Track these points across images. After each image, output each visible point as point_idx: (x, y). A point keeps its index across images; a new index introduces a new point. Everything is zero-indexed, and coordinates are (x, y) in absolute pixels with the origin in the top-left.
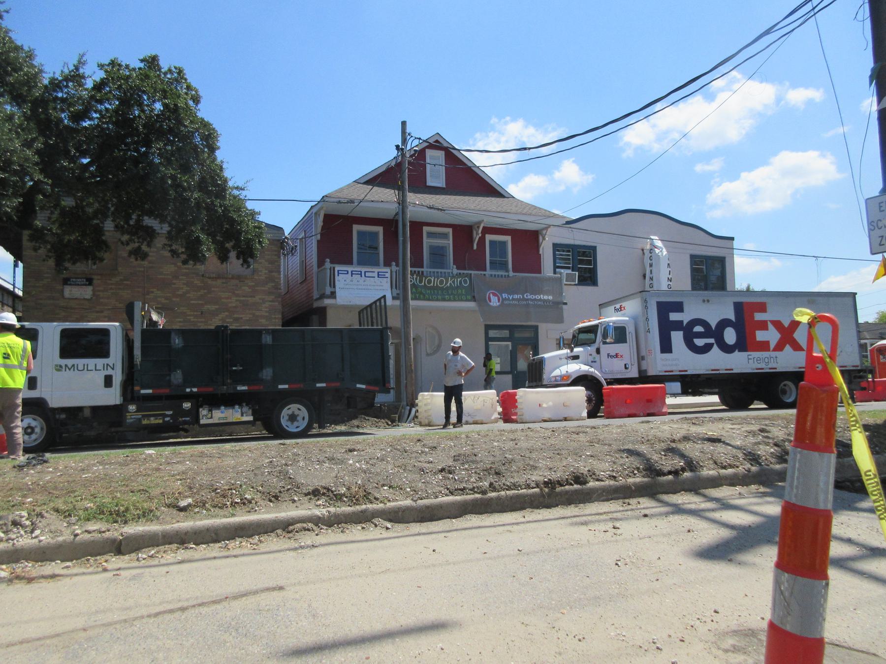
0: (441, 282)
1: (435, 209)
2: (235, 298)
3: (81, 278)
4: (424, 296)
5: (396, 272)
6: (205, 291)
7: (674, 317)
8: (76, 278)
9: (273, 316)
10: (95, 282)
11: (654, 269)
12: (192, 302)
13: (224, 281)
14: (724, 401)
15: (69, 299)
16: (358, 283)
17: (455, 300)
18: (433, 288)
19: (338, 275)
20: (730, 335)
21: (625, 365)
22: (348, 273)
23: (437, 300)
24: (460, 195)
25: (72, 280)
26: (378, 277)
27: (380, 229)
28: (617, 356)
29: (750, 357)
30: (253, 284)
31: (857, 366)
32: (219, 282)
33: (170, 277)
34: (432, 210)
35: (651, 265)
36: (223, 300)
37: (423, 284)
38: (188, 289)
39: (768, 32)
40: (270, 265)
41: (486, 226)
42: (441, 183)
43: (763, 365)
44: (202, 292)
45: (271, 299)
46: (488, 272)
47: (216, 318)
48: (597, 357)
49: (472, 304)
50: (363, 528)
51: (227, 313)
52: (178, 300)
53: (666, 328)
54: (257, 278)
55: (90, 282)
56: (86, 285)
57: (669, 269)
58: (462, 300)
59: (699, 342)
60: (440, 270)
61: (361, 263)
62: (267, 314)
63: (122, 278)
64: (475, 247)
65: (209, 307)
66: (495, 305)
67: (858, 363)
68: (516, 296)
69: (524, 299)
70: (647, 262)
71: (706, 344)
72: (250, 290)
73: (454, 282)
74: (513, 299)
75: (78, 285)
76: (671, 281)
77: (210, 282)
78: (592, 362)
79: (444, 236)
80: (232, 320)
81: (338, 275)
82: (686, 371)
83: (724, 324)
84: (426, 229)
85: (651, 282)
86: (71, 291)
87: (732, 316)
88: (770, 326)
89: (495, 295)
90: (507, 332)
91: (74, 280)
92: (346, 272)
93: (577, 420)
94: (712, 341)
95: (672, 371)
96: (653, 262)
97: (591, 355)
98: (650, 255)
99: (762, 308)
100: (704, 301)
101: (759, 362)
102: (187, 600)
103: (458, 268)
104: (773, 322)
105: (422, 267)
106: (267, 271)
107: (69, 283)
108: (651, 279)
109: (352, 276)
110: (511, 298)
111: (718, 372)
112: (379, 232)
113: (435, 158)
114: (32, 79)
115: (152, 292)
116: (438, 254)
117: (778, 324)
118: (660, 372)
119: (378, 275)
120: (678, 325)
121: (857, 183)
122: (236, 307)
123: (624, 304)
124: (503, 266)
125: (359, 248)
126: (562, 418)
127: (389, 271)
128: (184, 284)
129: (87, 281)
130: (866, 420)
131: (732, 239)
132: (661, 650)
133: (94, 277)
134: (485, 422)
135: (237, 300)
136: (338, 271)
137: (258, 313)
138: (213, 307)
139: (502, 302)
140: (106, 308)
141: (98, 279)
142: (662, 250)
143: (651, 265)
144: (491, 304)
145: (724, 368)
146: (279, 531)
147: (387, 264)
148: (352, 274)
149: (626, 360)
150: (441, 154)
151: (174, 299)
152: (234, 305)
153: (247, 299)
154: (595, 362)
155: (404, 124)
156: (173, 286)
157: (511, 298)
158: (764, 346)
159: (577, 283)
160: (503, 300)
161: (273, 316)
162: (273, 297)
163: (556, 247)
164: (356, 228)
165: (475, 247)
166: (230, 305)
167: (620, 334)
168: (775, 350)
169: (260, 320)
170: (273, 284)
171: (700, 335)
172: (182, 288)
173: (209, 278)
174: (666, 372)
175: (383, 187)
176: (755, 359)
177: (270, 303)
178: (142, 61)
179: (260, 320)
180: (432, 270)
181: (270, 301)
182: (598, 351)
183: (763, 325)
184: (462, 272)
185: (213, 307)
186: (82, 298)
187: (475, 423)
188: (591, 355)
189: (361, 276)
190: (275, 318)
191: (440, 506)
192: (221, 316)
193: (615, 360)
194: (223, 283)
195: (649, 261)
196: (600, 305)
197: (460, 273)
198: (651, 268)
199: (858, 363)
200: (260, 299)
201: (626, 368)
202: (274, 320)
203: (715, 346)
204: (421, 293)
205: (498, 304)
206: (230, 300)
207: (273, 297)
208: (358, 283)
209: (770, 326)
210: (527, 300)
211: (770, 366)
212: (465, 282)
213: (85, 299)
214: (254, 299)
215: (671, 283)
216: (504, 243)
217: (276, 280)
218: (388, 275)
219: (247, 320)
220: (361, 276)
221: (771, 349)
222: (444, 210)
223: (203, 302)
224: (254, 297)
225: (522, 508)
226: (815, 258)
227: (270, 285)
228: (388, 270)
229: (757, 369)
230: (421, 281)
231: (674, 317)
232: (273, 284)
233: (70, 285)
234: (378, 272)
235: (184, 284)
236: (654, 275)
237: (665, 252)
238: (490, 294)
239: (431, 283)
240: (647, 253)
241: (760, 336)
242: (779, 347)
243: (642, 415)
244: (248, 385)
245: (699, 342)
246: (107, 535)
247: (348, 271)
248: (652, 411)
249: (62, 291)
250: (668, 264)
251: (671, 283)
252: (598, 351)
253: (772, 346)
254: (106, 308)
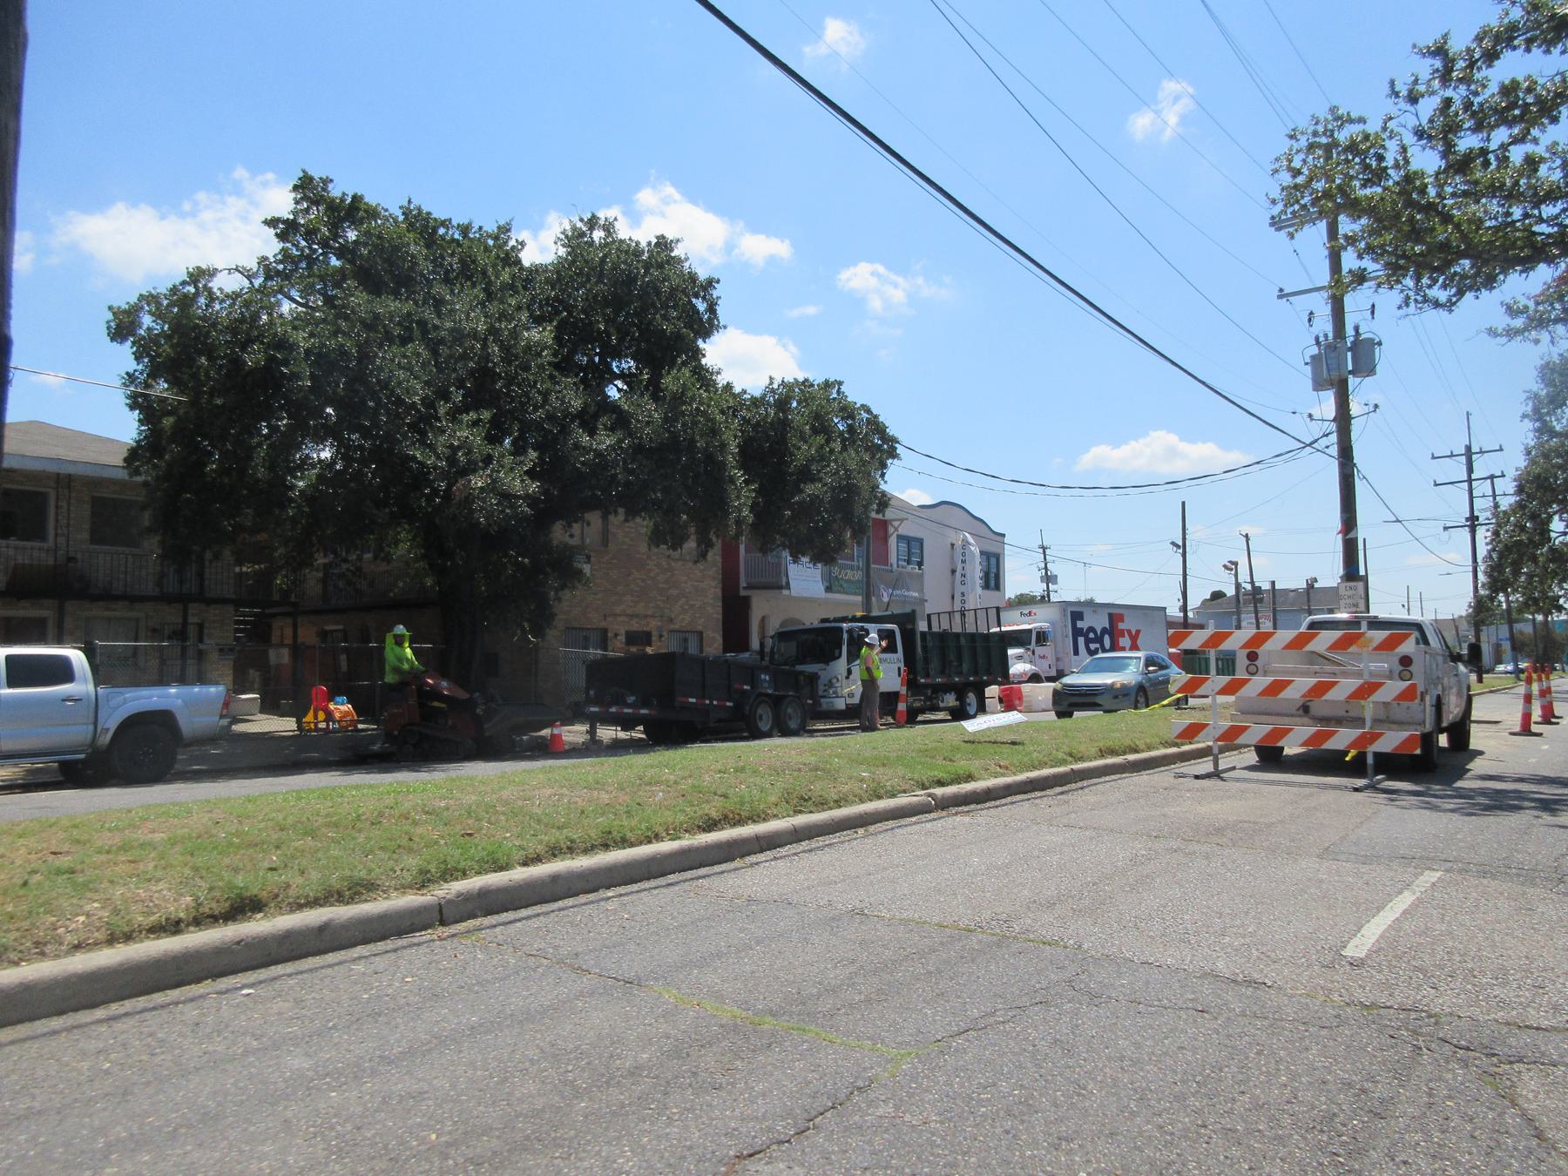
11: (967, 566)
12: (661, 586)
20: (1107, 641)
35: (963, 562)
53: (1077, 632)
70: (959, 558)
122: (690, 593)
131: (1004, 535)
138: (674, 592)
143: (963, 562)
158: (1123, 649)
167: (1042, 637)
185: (674, 592)
240: (958, 550)
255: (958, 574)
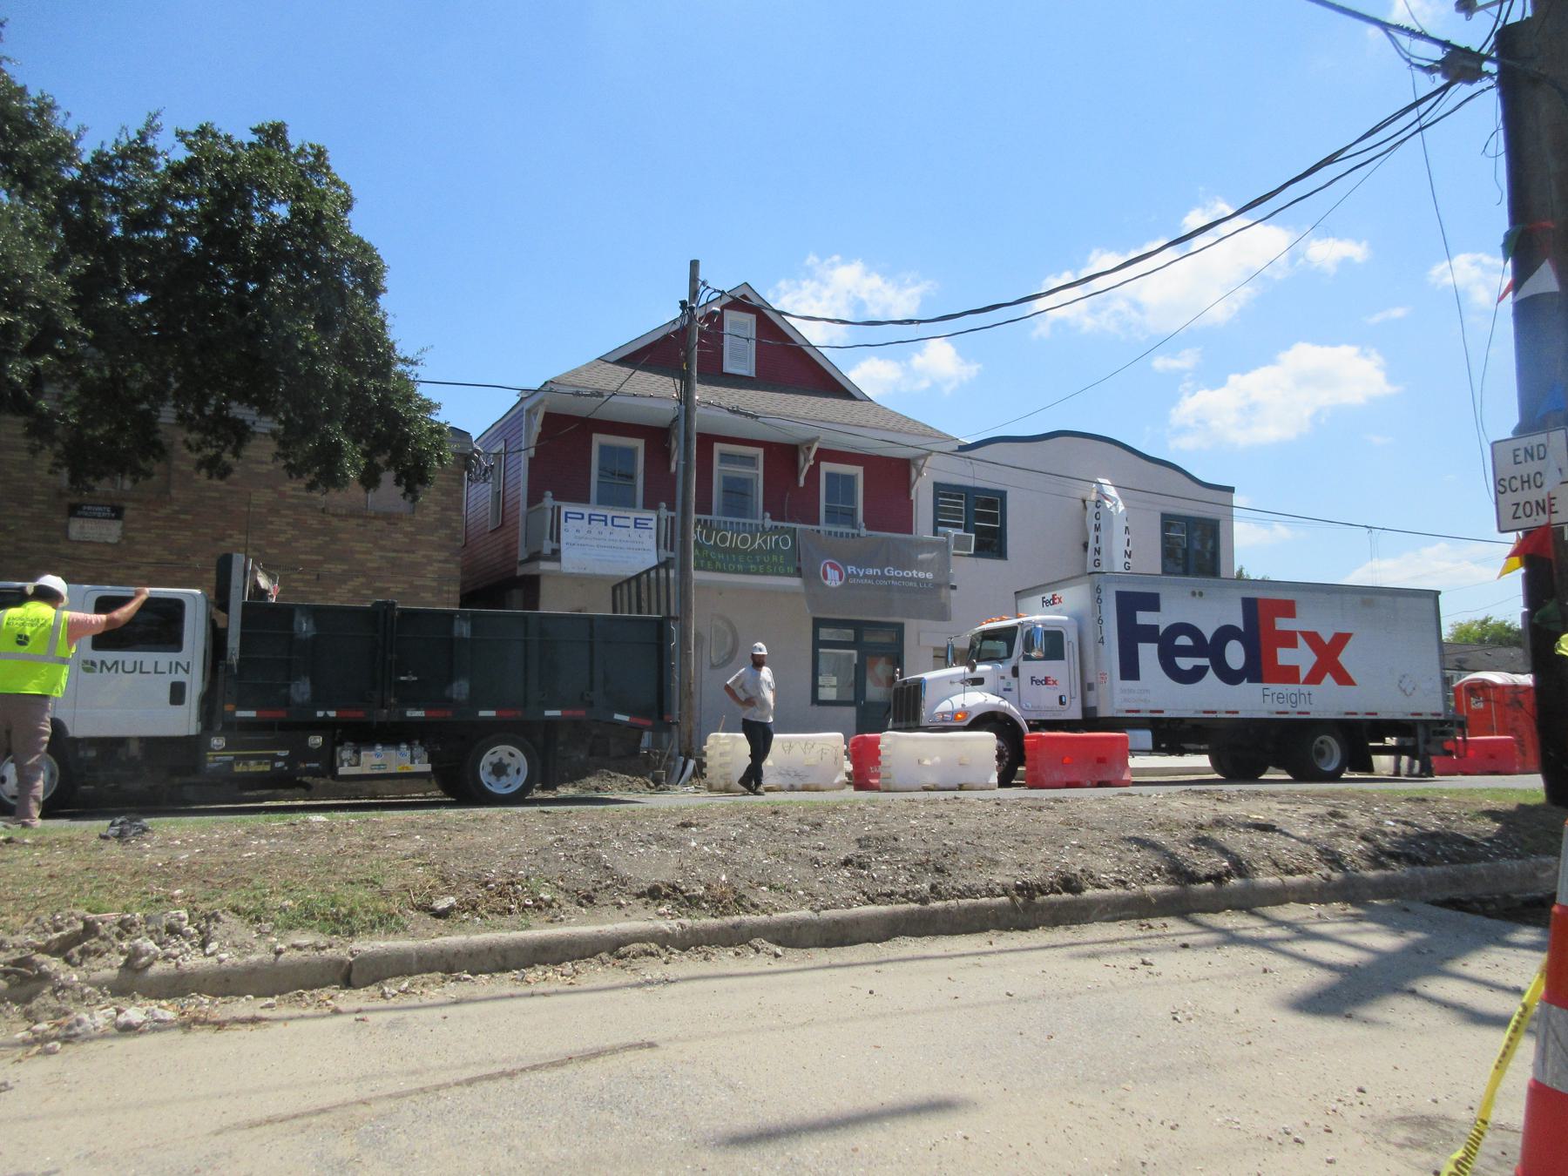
0: (744, 541)
1: (741, 413)
2: (382, 554)
3: (103, 506)
4: (714, 563)
5: (667, 520)
6: (327, 539)
7: (1144, 618)
8: (93, 505)
9: (445, 588)
10: (127, 513)
11: (1102, 534)
12: (303, 557)
13: (361, 521)
14: (1217, 765)
15: (79, 542)
16: (601, 537)
17: (765, 573)
18: (726, 551)
19: (566, 521)
20: (1235, 655)
21: (1061, 697)
22: (583, 518)
23: (736, 572)
24: (781, 392)
25: (85, 508)
26: (635, 527)
27: (639, 444)
28: (1046, 680)
29: (1266, 692)
30: (412, 529)
31: (1439, 715)
32: (353, 522)
33: (264, 510)
34: (737, 417)
35: (1097, 528)
36: (358, 556)
37: (712, 542)
38: (297, 533)
39: (1329, 160)
40: (444, 498)
41: (822, 446)
42: (747, 368)
43: (1288, 707)
44: (321, 540)
45: (443, 558)
46: (823, 527)
47: (343, 586)
48: (1014, 682)
49: (795, 582)
50: (737, 954)
51: (362, 580)
52: (276, 551)
53: (1131, 634)
54: (420, 518)
55: (117, 513)
56: (111, 518)
57: (1128, 536)
58: (778, 574)
59: (1185, 663)
60: (736, 520)
61: (603, 501)
62: (435, 584)
63: (177, 508)
64: (802, 482)
65: (330, 566)
66: (833, 585)
67: (1440, 709)
68: (870, 572)
69: (883, 577)
70: (1091, 522)
71: (1196, 667)
72: (407, 540)
73: (765, 542)
74: (865, 576)
75: (96, 517)
76: (1129, 557)
77: (335, 522)
78: (1005, 690)
79: (750, 461)
80: (370, 592)
81: (566, 521)
82: (1162, 712)
83: (1226, 633)
84: (718, 447)
85: (1097, 557)
86: (82, 527)
87: (1239, 622)
88: (1300, 640)
89: (834, 567)
90: (851, 632)
91: (89, 508)
92: (580, 516)
93: (982, 789)
94: (1205, 661)
95: (1138, 711)
96: (1101, 521)
97: (1003, 678)
98: (1096, 510)
99: (1288, 609)
100: (1194, 594)
101: (1281, 700)
102: (505, 1061)
103: (773, 518)
104: (1305, 635)
105: (710, 514)
106: (438, 509)
107: (79, 513)
108: (1098, 551)
109: (590, 523)
110: (861, 574)
111: (1214, 716)
112: (637, 448)
113: (739, 326)
114: (63, 150)
115: (231, 536)
116: (737, 492)
117: (1312, 639)
118: (1118, 711)
119: (636, 523)
120: (1150, 633)
121: (1479, 417)
122: (378, 569)
123: (1059, 593)
124: (848, 517)
125: (600, 475)
126: (955, 785)
127: (655, 518)
128: (288, 524)
129: (112, 511)
130: (1489, 804)
131: (1231, 490)
132: (1302, 1143)
133: (126, 504)
134: (822, 787)
135: (382, 557)
136: (566, 513)
137: (418, 582)
138: (338, 568)
139: (847, 580)
140: (145, 560)
141: (133, 509)
142: (1116, 505)
143: (1097, 528)
144: (828, 583)
145: (1223, 708)
146: (604, 955)
147: (650, 504)
148: (590, 520)
149: (1062, 689)
150: (749, 319)
151: (268, 551)
152: (375, 565)
153: (400, 555)
154: (1010, 690)
155: (694, 265)
156: (270, 527)
157: (861, 574)
158: (1290, 674)
159: (972, 552)
160: (849, 576)
161: (445, 588)
162: (447, 554)
163: (940, 490)
164: (598, 439)
165: (802, 482)
166: (370, 565)
167: (1054, 644)
168: (1307, 681)
169: (422, 595)
170: (448, 532)
171: (1186, 652)
172: (285, 532)
173: (334, 515)
174: (1128, 711)
175: (649, 371)
176: (1275, 696)
177: (441, 565)
178: (255, 131)
179: (422, 595)
180: (724, 519)
181: (440, 562)
182: (1015, 672)
183: (1289, 640)
184: (780, 524)
186: (102, 541)
187: (806, 789)
188: (1003, 678)
189: (606, 524)
190: (449, 592)
191: (857, 922)
192: (351, 585)
193: (1044, 688)
194: (358, 525)
195: (1095, 521)
196: (1016, 593)
197: (776, 527)
198: (1097, 533)
199: (1440, 709)
200: (424, 556)
201: (1061, 703)
202: (446, 596)
203: (1211, 669)
204: (708, 558)
205: (839, 583)
206: (369, 557)
207: (447, 554)
208: (601, 537)
209: (1300, 640)
210: (890, 578)
211: (1299, 709)
212: (785, 542)
213: (107, 544)
214: (412, 556)
215: (1129, 561)
216: (850, 479)
217: (454, 525)
218: (653, 524)
219: (399, 593)
220: (606, 524)
221: (1301, 681)
222: (757, 417)
223: (321, 558)
224: (413, 552)
225: (983, 929)
226: (1368, 530)
227: (443, 532)
228: (652, 515)
229: (1278, 713)
230: (708, 538)
231: (1144, 618)
232: (448, 532)
233: (82, 516)
234: (636, 519)
235: (288, 524)
236: (1103, 545)
237: (1121, 508)
238: (825, 566)
239: (742, 538)
240: (1091, 506)
241: (1285, 656)
242: (1315, 677)
243: (1089, 783)
244: (426, 709)
245: (1185, 663)
246: (329, 953)
247: (583, 515)
248: (1106, 778)
249: (66, 528)
250: (1127, 528)
251: (1129, 561)
252: (1015, 672)
253: (1303, 674)
254: (145, 560)
255: (1091, 546)
